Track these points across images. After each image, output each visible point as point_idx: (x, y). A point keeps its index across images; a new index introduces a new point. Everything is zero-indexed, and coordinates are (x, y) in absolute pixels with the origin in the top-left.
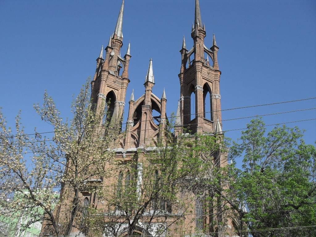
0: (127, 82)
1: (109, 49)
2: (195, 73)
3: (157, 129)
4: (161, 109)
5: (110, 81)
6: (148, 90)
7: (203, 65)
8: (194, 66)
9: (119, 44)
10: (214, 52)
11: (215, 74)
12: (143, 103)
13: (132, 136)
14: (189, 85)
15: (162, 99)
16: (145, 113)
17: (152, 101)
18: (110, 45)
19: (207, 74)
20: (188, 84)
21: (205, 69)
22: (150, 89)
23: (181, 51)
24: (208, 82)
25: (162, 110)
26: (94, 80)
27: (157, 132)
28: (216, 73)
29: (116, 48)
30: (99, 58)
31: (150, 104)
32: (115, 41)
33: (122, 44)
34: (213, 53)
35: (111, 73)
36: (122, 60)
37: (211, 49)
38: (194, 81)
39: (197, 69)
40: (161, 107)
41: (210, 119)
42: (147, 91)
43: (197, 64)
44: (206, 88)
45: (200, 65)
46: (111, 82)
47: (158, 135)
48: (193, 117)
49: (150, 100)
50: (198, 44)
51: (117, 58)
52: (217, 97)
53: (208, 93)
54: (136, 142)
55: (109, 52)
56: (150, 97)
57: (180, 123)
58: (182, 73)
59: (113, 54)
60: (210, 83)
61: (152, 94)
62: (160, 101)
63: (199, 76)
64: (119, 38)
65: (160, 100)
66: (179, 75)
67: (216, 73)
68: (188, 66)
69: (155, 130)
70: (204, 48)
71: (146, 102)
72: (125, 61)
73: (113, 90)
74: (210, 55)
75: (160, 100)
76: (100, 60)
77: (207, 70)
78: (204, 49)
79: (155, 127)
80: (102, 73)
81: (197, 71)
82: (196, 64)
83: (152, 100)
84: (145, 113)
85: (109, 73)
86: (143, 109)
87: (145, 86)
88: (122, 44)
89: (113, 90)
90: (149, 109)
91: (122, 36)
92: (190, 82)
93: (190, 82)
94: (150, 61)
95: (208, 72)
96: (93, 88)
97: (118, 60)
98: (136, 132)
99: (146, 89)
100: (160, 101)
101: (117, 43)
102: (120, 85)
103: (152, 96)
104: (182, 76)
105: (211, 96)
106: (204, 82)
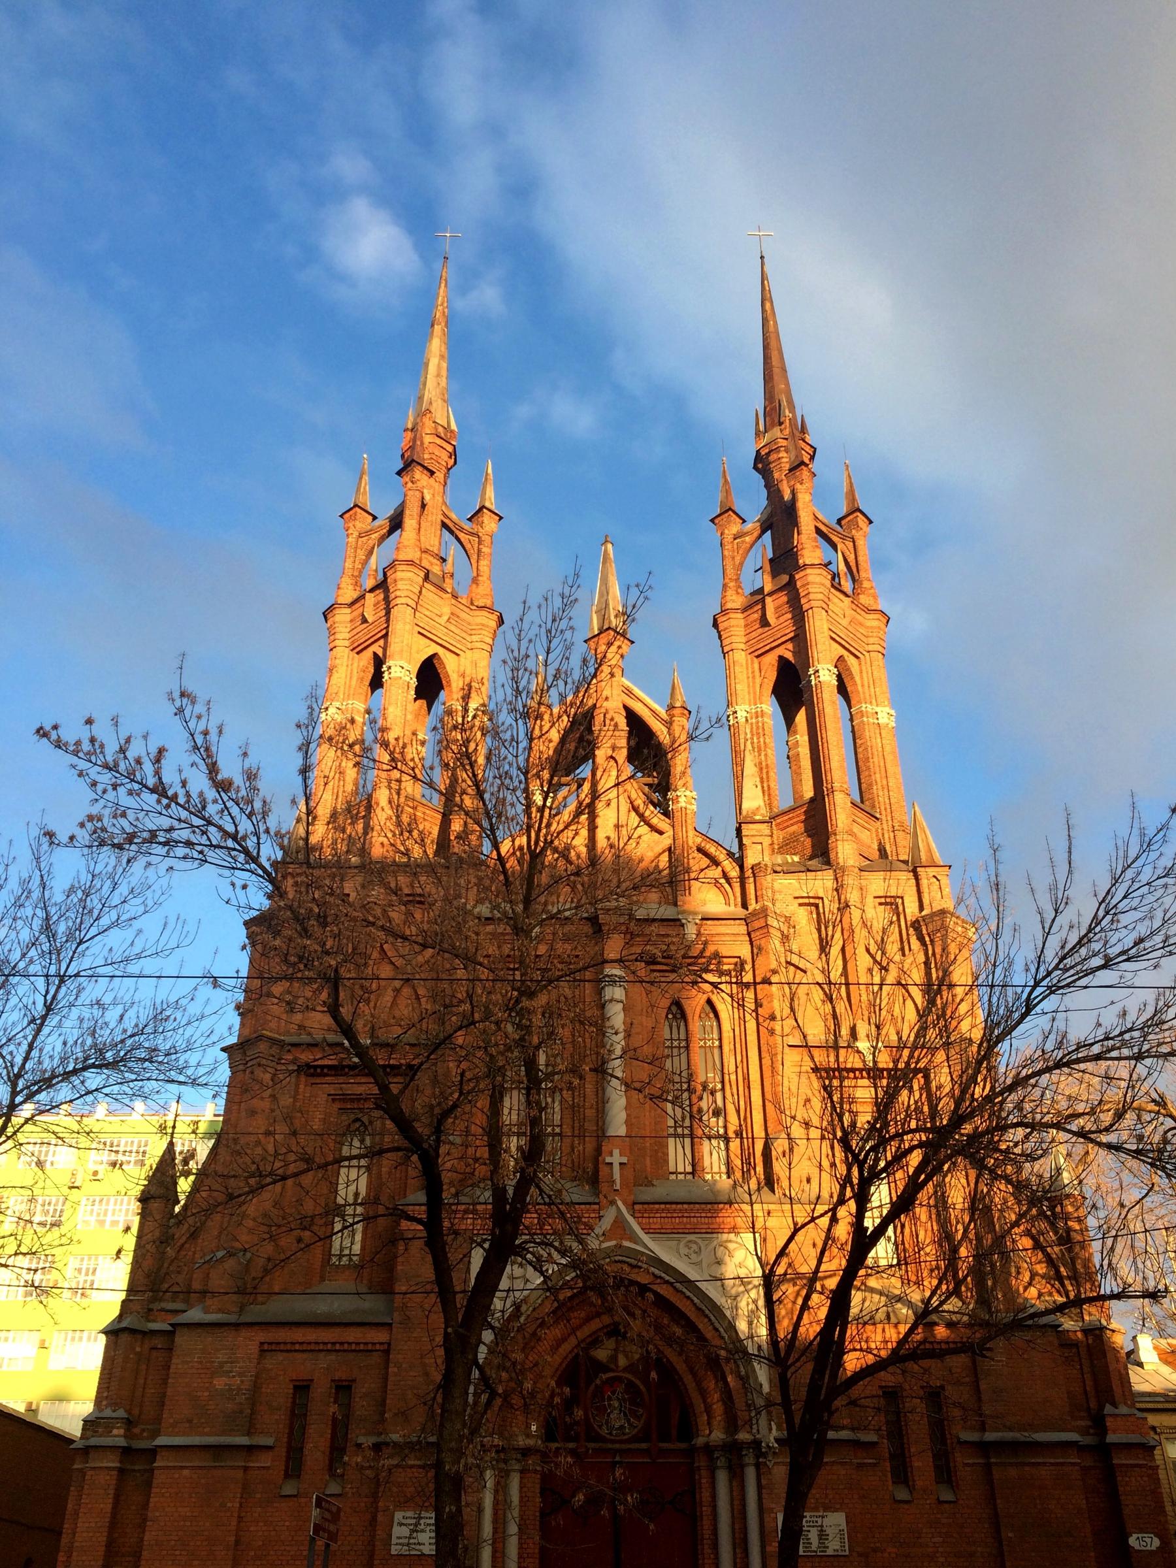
5: (427, 613)
8: (799, 584)
11: (869, 624)
21: (836, 600)
31: (622, 722)
33: (455, 463)
46: (433, 616)
52: (883, 719)
57: (763, 811)
60: (852, 657)
73: (441, 651)
77: (841, 604)
83: (625, 707)
88: (455, 463)
89: (441, 651)
102: (464, 635)
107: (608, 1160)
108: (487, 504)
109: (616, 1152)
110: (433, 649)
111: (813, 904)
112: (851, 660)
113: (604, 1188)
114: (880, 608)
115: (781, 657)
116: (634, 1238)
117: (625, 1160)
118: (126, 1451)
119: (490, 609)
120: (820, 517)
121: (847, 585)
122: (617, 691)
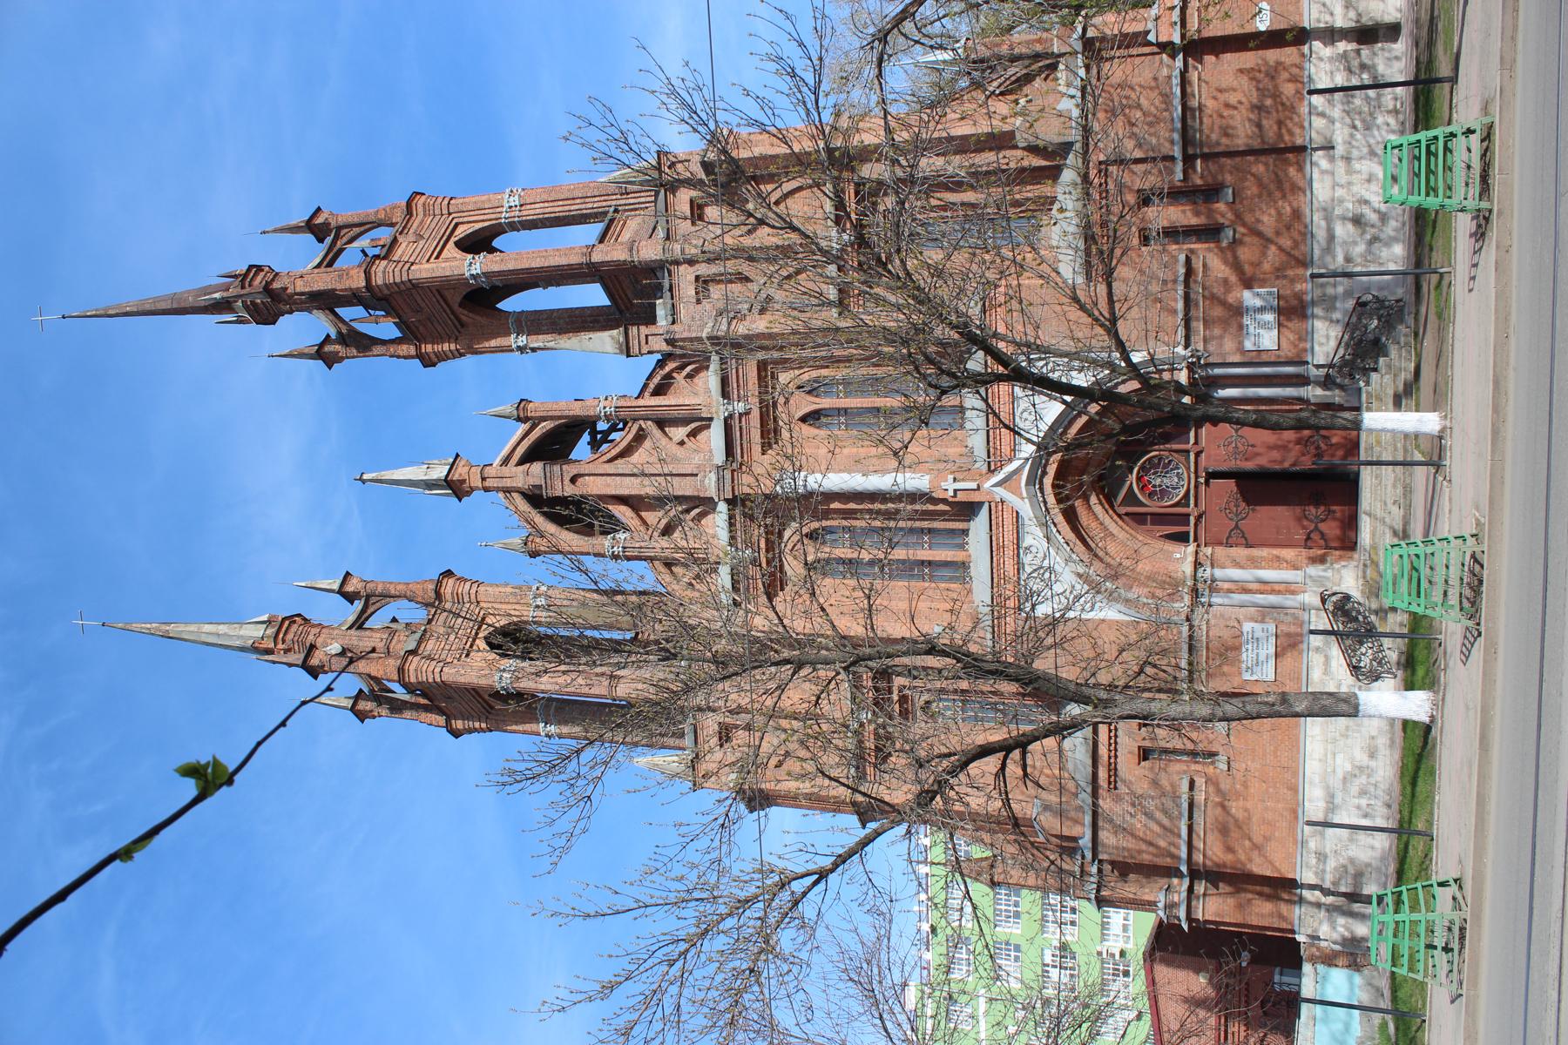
0: (451, 581)
1: (314, 662)
2: (414, 287)
3: (641, 429)
4: (559, 418)
6: (483, 479)
7: (384, 258)
8: (386, 292)
9: (294, 627)
10: (333, 224)
12: (535, 498)
13: (667, 531)
14: (465, 315)
15: (519, 419)
16: (573, 480)
17: (528, 458)
18: (297, 658)
19: (422, 243)
20: (462, 325)
21: (399, 252)
22: (476, 471)
23: (330, 361)
24: (453, 239)
25: (566, 413)
26: (442, 720)
27: (650, 426)
28: (420, 209)
29: (311, 637)
30: (352, 709)
31: (537, 467)
32: (280, 646)
34: (339, 228)
35: (412, 646)
36: (363, 611)
37: (321, 240)
38: (446, 293)
39: (398, 280)
40: (552, 418)
41: (596, 229)
42: (487, 484)
43: (378, 280)
44: (478, 243)
45: (381, 268)
47: (661, 423)
48: (593, 296)
49: (521, 468)
50: (299, 283)
51: (352, 632)
53: (495, 243)
54: (694, 512)
55: (325, 659)
56: (511, 469)
58: (418, 348)
59: (335, 648)
61: (497, 462)
62: (526, 426)
63: (426, 270)
64: (271, 631)
65: (523, 428)
66: (428, 362)
67: (420, 209)
68: (386, 329)
69: (640, 437)
70: (318, 266)
71: (532, 481)
72: (368, 597)
74: (345, 239)
75: (523, 428)
76: (364, 705)
78: (322, 269)
79: (630, 436)
80: (413, 680)
81: (405, 278)
82: (380, 282)
83: (521, 463)
84: (573, 480)
85: (413, 652)
86: (558, 493)
87: (468, 493)
90: (556, 468)
91: (265, 618)
92: (453, 313)
93: (453, 313)
94: (364, 482)
95: (411, 237)
96: (477, 725)
97: (360, 627)
98: (651, 517)
99: (477, 488)
100: (526, 426)
101: (290, 636)
103: (505, 462)
104: (429, 348)
105: (513, 227)
106: (451, 250)
107: (951, 493)
108: (336, 587)
109: (944, 485)
110: (481, 644)
111: (703, 283)
112: (461, 232)
113: (976, 497)
114: (404, 203)
115: (460, 305)
116: (1018, 471)
117: (951, 477)
118: (1195, 874)
119: (439, 582)
120: (318, 260)
121: (384, 234)
122: (506, 471)
